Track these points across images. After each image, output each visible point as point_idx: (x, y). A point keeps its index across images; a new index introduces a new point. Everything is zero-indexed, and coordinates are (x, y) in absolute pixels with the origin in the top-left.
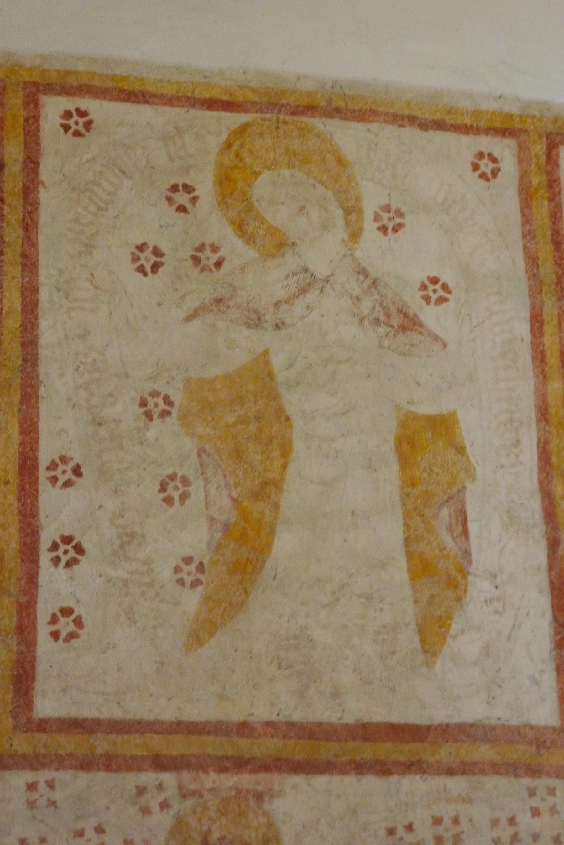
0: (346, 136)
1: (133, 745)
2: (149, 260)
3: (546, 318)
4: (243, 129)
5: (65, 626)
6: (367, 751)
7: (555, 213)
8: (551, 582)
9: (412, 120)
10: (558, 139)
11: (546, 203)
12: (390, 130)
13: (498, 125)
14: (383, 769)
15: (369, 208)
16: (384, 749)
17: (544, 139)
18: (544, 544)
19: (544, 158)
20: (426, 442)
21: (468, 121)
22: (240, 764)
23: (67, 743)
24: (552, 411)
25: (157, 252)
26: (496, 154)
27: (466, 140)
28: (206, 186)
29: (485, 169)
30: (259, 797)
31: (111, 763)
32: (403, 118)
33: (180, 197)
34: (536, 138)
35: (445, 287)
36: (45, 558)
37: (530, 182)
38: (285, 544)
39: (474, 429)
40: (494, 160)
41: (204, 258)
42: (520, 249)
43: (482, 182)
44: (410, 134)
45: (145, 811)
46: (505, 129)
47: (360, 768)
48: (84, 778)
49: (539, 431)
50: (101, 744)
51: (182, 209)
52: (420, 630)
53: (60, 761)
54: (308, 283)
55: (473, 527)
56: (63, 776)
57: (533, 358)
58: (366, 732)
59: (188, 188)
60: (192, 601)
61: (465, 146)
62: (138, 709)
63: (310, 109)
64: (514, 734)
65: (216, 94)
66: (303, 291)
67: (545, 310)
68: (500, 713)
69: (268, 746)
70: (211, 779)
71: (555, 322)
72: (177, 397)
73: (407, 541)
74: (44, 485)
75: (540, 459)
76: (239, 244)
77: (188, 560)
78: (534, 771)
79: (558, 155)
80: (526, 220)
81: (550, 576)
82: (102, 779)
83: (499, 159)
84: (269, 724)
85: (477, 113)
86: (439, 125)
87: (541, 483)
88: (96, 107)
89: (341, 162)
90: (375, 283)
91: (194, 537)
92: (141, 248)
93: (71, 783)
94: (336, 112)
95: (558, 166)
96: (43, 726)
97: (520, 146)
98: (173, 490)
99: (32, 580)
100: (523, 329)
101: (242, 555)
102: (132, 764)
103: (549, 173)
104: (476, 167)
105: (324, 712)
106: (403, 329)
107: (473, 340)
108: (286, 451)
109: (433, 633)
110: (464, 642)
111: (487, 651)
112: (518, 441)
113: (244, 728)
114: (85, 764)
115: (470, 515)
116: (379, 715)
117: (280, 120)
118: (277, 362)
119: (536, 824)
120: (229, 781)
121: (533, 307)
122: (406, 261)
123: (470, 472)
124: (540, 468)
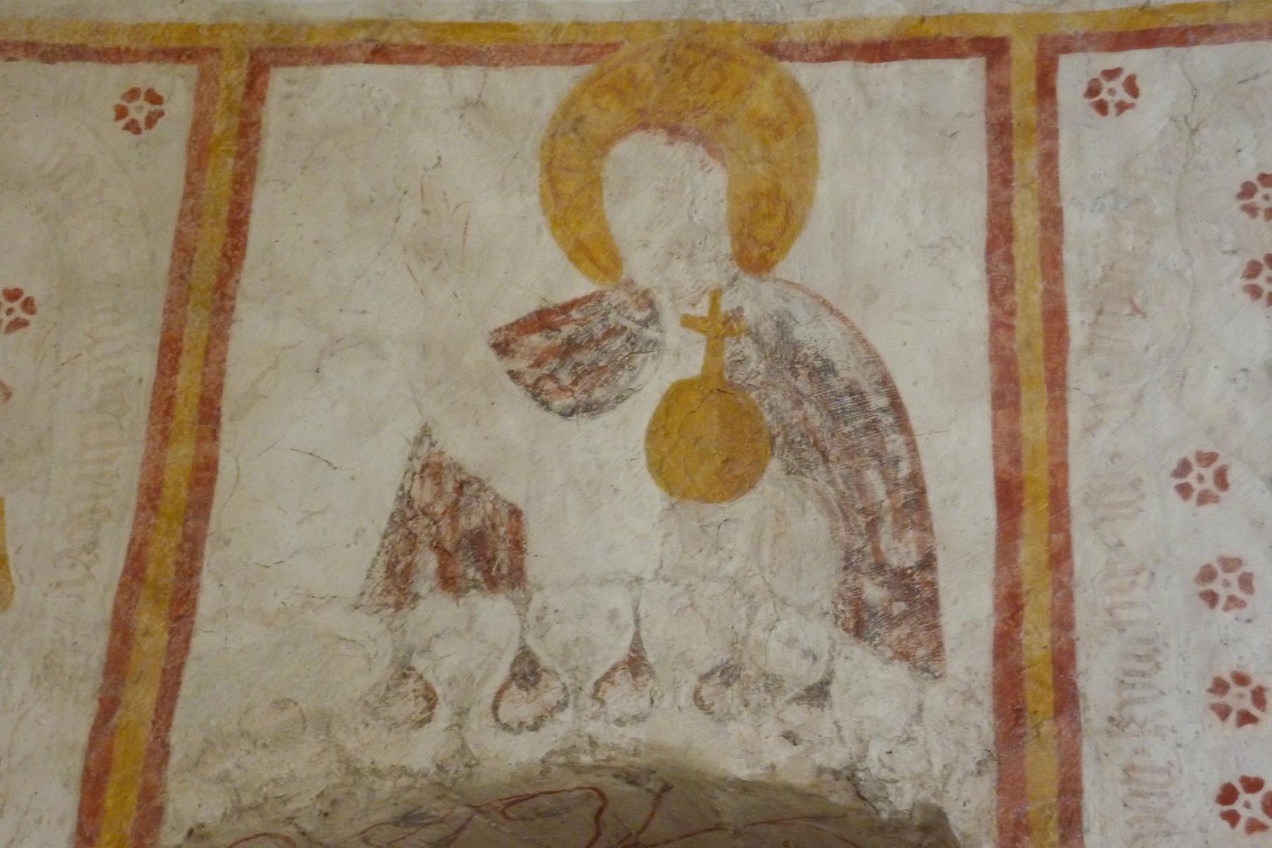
3: (186, 344)
7: (242, 175)
8: (87, 770)
9: (32, 49)
10: (269, 58)
11: (231, 161)
13: (174, 44)
17: (247, 59)
18: (92, 708)
19: (242, 89)
21: (123, 42)
24: (167, 492)
26: (159, 91)
32: (16, 46)
34: (233, 59)
35: (29, 305)
37: (211, 129)
40: (154, 98)
42: (170, 237)
43: (129, 136)
46: (180, 49)
49: (136, 525)
57: (152, 409)
61: (111, 81)
67: (187, 331)
71: (201, 350)
75: (125, 572)
79: (266, 83)
80: (192, 189)
81: (87, 758)
83: (166, 98)
85: (138, 30)
86: (77, 53)
87: (117, 609)
95: (262, 100)
97: (203, 77)
100: (144, 365)
103: (244, 113)
104: (121, 113)
107: (57, 386)
112: (95, 543)
121: (167, 328)
124: (122, 585)
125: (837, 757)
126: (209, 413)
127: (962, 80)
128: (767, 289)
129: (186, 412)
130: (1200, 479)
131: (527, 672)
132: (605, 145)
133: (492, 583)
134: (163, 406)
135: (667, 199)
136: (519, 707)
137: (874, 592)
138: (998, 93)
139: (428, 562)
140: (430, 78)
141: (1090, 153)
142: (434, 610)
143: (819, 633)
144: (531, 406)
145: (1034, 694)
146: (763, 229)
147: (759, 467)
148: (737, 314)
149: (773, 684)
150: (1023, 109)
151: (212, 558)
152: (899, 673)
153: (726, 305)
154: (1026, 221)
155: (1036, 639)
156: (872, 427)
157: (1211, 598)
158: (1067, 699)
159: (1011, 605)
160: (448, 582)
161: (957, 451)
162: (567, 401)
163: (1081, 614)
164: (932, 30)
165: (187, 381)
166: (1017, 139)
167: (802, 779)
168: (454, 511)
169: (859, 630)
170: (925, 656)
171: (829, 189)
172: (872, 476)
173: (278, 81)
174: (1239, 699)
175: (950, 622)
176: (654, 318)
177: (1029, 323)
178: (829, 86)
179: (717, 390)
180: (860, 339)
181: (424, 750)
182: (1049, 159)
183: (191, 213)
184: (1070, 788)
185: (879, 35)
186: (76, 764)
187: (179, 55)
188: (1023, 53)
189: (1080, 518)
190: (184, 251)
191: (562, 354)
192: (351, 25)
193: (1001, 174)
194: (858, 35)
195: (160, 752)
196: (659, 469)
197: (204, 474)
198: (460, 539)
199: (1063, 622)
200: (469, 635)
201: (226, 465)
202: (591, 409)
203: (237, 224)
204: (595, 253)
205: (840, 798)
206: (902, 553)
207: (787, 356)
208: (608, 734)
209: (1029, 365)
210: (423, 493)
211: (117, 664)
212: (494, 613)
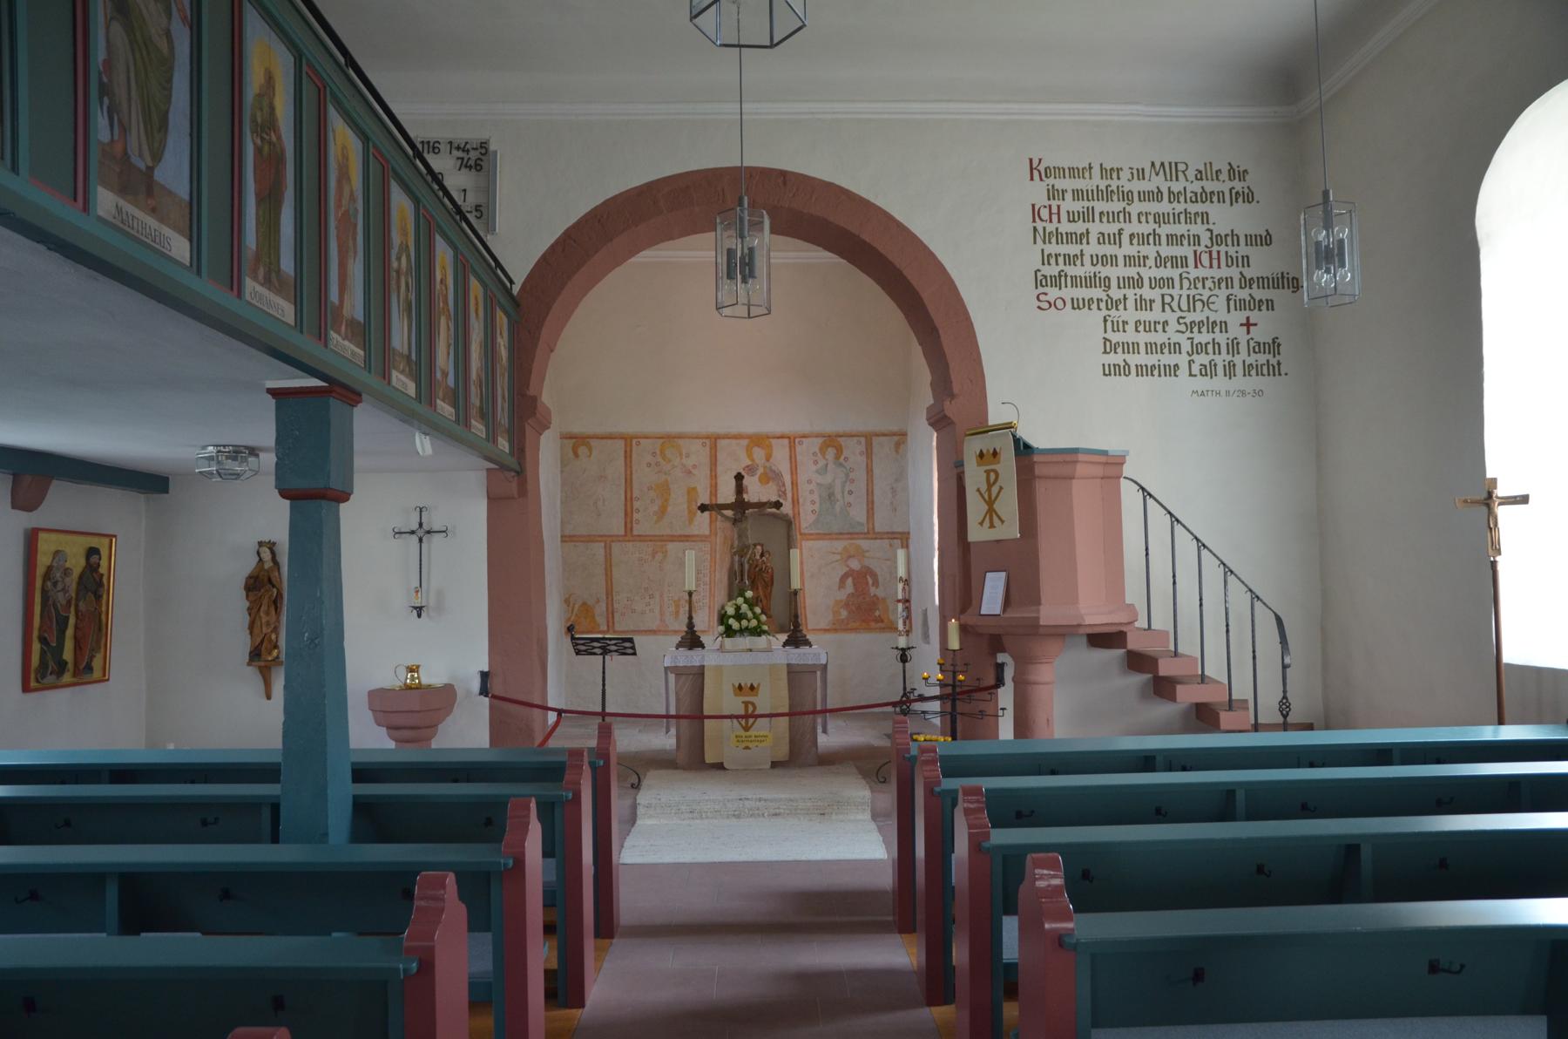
0: (681, 442)
2: (649, 465)
29: (704, 445)
33: (654, 454)
41: (657, 464)
46: (708, 437)
98: (652, 501)
101: (662, 512)
122: (689, 462)
127: (786, 441)
130: (809, 482)
135: (759, 454)
141: (798, 449)
145: (795, 502)
161: (787, 479)
166: (792, 448)
178: (774, 441)
179: (765, 474)
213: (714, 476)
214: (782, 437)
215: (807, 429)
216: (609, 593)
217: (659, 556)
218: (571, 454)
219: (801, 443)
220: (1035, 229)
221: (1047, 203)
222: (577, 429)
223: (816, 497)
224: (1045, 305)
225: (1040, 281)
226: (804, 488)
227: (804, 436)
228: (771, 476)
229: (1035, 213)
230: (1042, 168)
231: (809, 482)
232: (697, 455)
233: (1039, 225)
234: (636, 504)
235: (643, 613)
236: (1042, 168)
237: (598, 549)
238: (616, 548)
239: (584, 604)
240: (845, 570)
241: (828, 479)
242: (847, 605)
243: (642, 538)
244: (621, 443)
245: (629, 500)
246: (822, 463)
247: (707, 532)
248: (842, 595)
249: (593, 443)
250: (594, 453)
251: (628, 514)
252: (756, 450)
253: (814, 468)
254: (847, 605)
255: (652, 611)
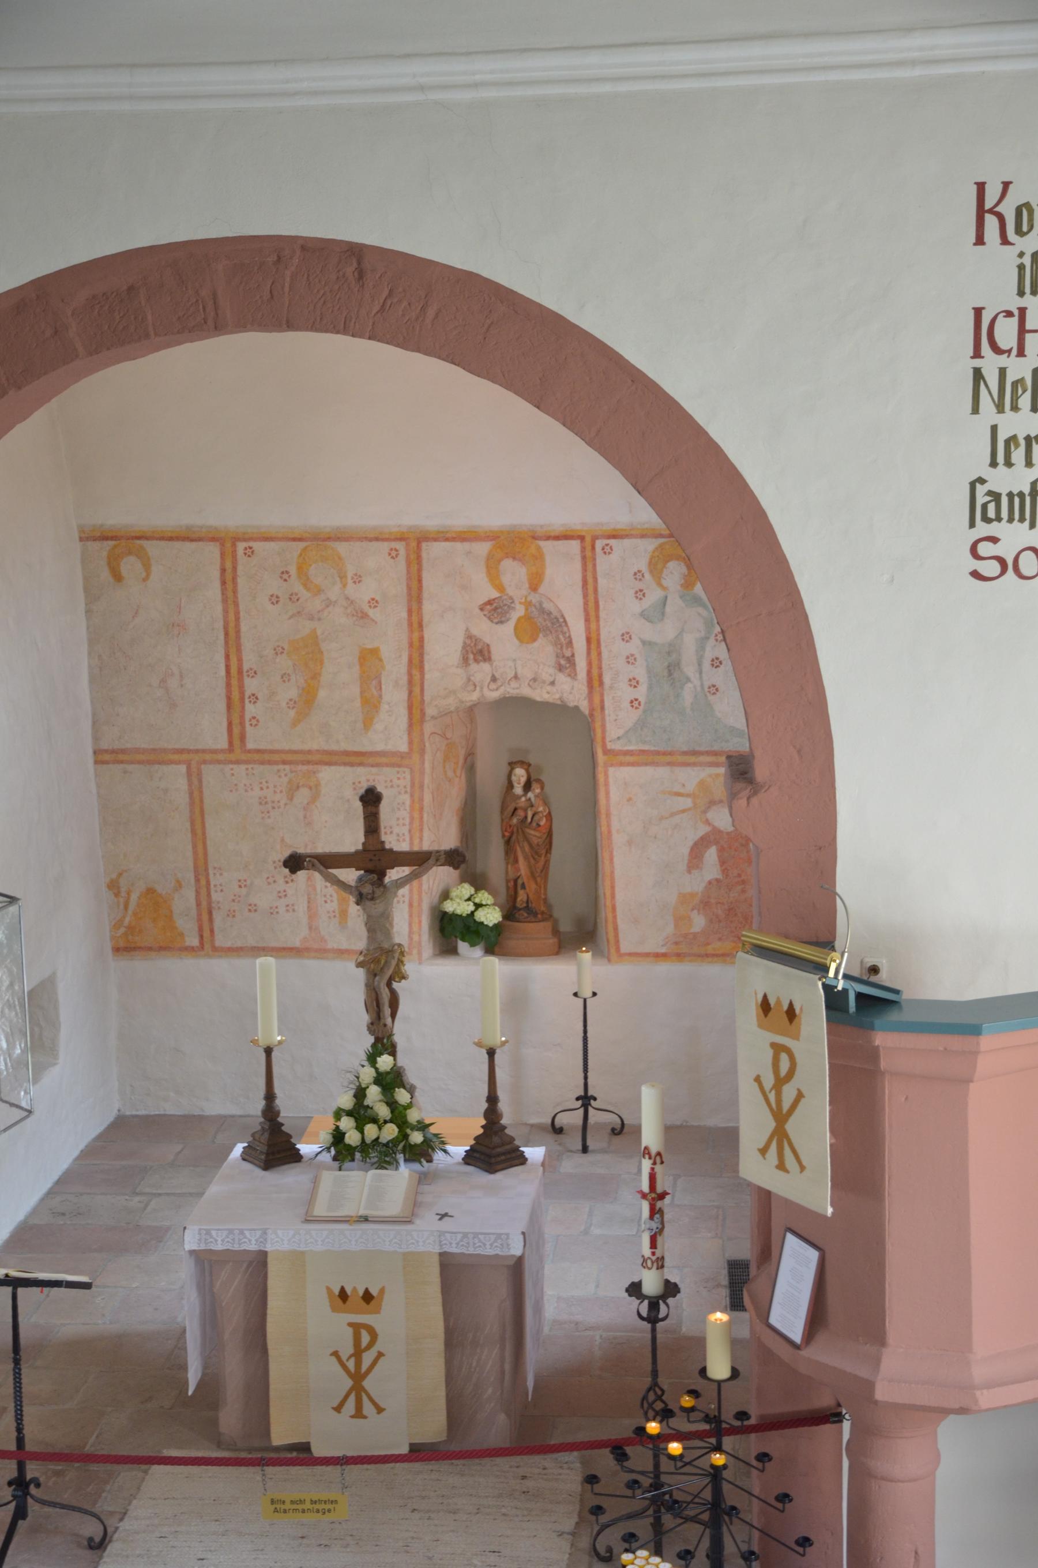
0: (342, 548)
1: (276, 757)
2: (275, 600)
4: (305, 548)
5: (254, 722)
6: (347, 759)
12: (358, 544)
14: (352, 765)
15: (350, 575)
16: (353, 759)
20: (369, 657)
22: (309, 762)
23: (257, 757)
25: (277, 597)
27: (386, 544)
28: (293, 570)
29: (393, 554)
30: (314, 773)
31: (270, 763)
33: (285, 576)
36: (247, 701)
38: (322, 694)
39: (386, 652)
40: (396, 550)
41: (293, 598)
44: (364, 544)
45: (280, 777)
46: (401, 538)
47: (345, 764)
48: (262, 767)
50: (267, 757)
51: (285, 580)
52: (364, 723)
53: (254, 762)
54: (329, 603)
55: (383, 687)
56: (256, 766)
58: (347, 753)
59: (287, 572)
60: (292, 713)
61: (385, 546)
62: (277, 746)
63: (329, 539)
64: (394, 754)
65: (296, 535)
66: (328, 606)
68: (389, 747)
69: (317, 757)
70: (300, 767)
72: (286, 647)
73: (361, 692)
74: (245, 677)
76: (305, 592)
77: (291, 700)
78: (399, 766)
80: (408, 572)
82: (267, 767)
84: (317, 751)
85: (390, 533)
86: (377, 539)
88: (255, 545)
89: (340, 558)
90: (352, 602)
91: (293, 693)
92: (272, 596)
93: (259, 769)
94: (338, 539)
96: (249, 751)
98: (285, 677)
99: (243, 708)
100: (404, 614)
101: (307, 700)
102: (276, 763)
105: (334, 747)
106: (362, 617)
108: (322, 663)
109: (368, 723)
110: (378, 726)
111: (386, 728)
113: (309, 752)
114: (262, 763)
115: (383, 682)
116: (350, 748)
117: (320, 541)
118: (319, 632)
119: (398, 782)
120: (305, 768)
122: (363, 593)
123: (383, 667)
125: (557, 696)
126: (421, 625)
127: (575, 545)
128: (537, 596)
129: (415, 626)
130: (626, 637)
131: (494, 679)
132: (500, 561)
133: (485, 660)
134: (410, 624)
136: (493, 686)
137: (563, 662)
138: (583, 549)
139: (471, 656)
140: (458, 545)
141: (603, 563)
142: (474, 667)
143: (552, 671)
144: (488, 621)
145: (595, 682)
146: (535, 583)
147: (538, 636)
148: (531, 602)
149: (544, 682)
150: (589, 554)
151: (426, 657)
152: (569, 679)
153: (529, 599)
154: (590, 580)
155: (595, 672)
156: (560, 626)
157: (628, 662)
158: (601, 683)
159: (590, 664)
160: (476, 661)
161: (577, 629)
162: (496, 620)
163: (604, 666)
164: (568, 533)
165: (415, 619)
166: (588, 561)
167: (551, 701)
168: (475, 645)
169: (560, 670)
170: (573, 675)
171: (549, 572)
172: (561, 636)
173: (424, 545)
174: (634, 683)
175: (578, 668)
176: (513, 602)
177: (591, 604)
178: (547, 546)
179: (527, 618)
180: (557, 606)
181: (475, 696)
182: (594, 565)
183: (409, 579)
184: (602, 701)
185: (557, 534)
186: (406, 704)
187: (401, 539)
188: (588, 539)
189: (603, 644)
190: (409, 588)
191: (495, 610)
192: (439, 532)
193: (584, 569)
194: (553, 534)
195: (423, 701)
196: (518, 638)
197: (421, 639)
198: (477, 652)
199: (600, 668)
200: (481, 671)
201: (426, 636)
202: (501, 622)
203: (420, 581)
204: (501, 588)
205: (559, 702)
206: (568, 654)
207: (542, 611)
208: (512, 691)
209: (592, 612)
210: (468, 642)
211: (410, 682)
212: (485, 666)
213: (416, 624)
214: (565, 536)
215: (621, 519)
216: (201, 870)
217: (303, 796)
218: (105, 574)
219: (607, 551)
220: (978, 375)
221: (1014, 303)
222: (116, 516)
223: (640, 672)
224: (991, 568)
225: (983, 507)
226: (614, 651)
227: (615, 535)
228: (540, 624)
229: (982, 333)
230: (1007, 208)
231: (626, 637)
232: (380, 575)
233: (990, 364)
234: (251, 685)
235: (273, 912)
236: (1007, 208)
237: (175, 779)
238: (211, 775)
239: (150, 891)
240: (703, 830)
241: (666, 632)
242: (705, 904)
243: (266, 757)
244: (212, 550)
245: (235, 675)
246: (654, 595)
247: (404, 748)
248: (696, 884)
249: (152, 548)
250: (154, 569)
251: (235, 701)
252: (507, 564)
253: (636, 607)
254: (705, 904)
255: (290, 908)
